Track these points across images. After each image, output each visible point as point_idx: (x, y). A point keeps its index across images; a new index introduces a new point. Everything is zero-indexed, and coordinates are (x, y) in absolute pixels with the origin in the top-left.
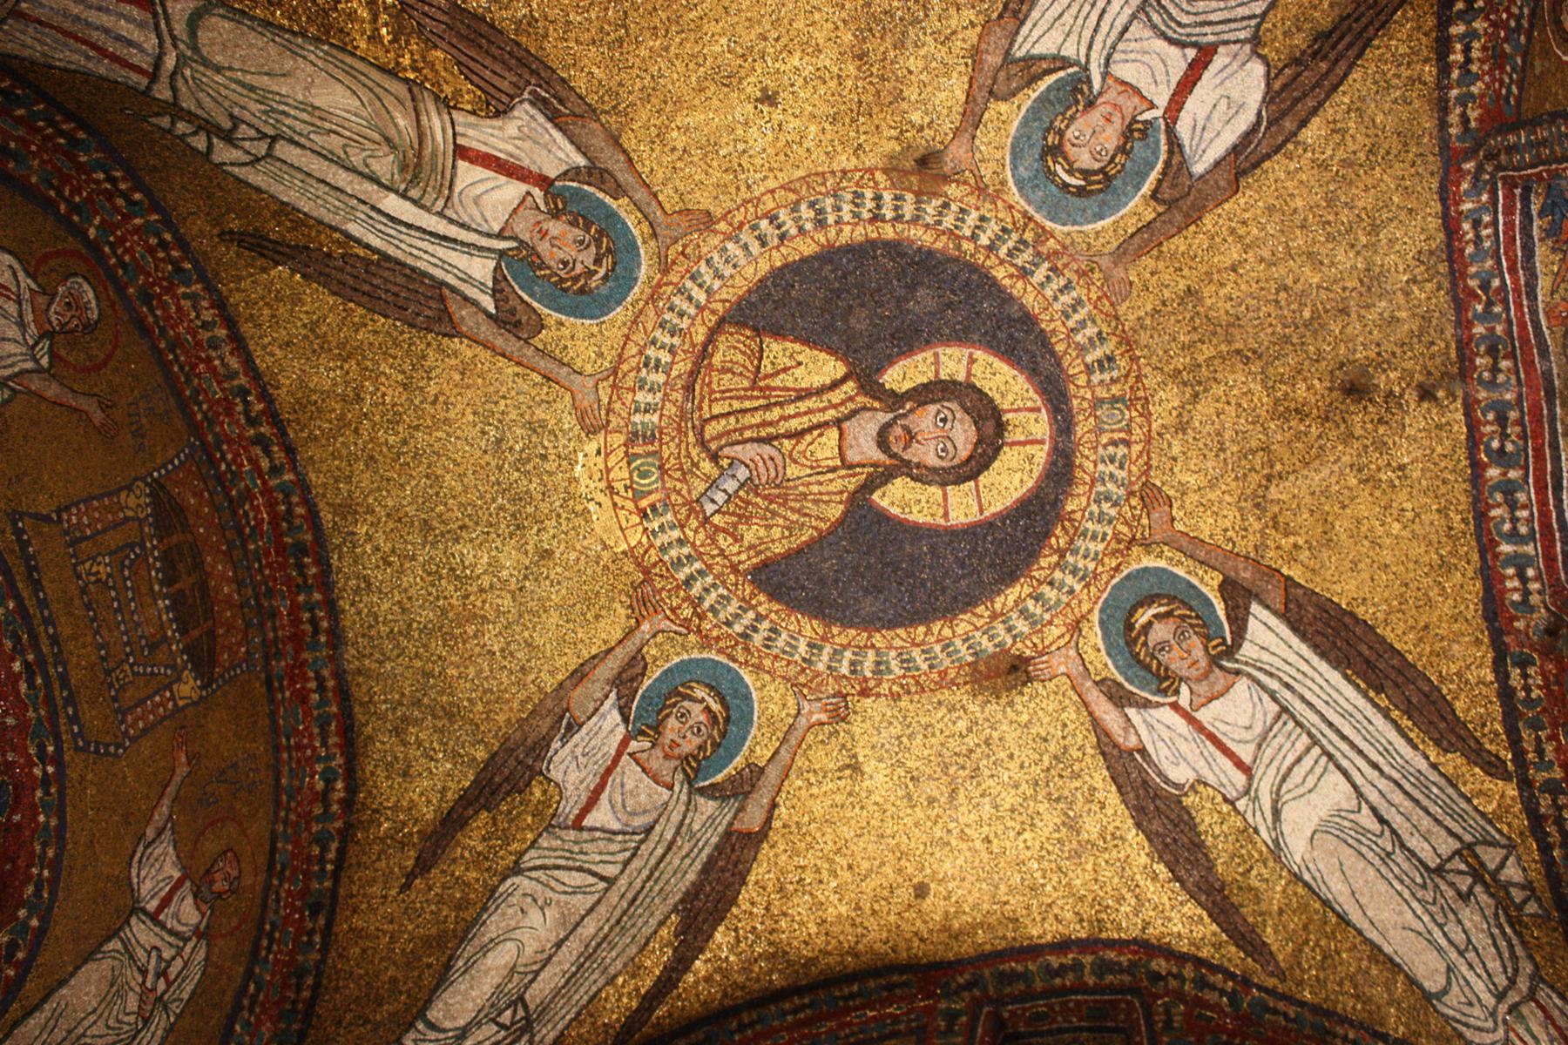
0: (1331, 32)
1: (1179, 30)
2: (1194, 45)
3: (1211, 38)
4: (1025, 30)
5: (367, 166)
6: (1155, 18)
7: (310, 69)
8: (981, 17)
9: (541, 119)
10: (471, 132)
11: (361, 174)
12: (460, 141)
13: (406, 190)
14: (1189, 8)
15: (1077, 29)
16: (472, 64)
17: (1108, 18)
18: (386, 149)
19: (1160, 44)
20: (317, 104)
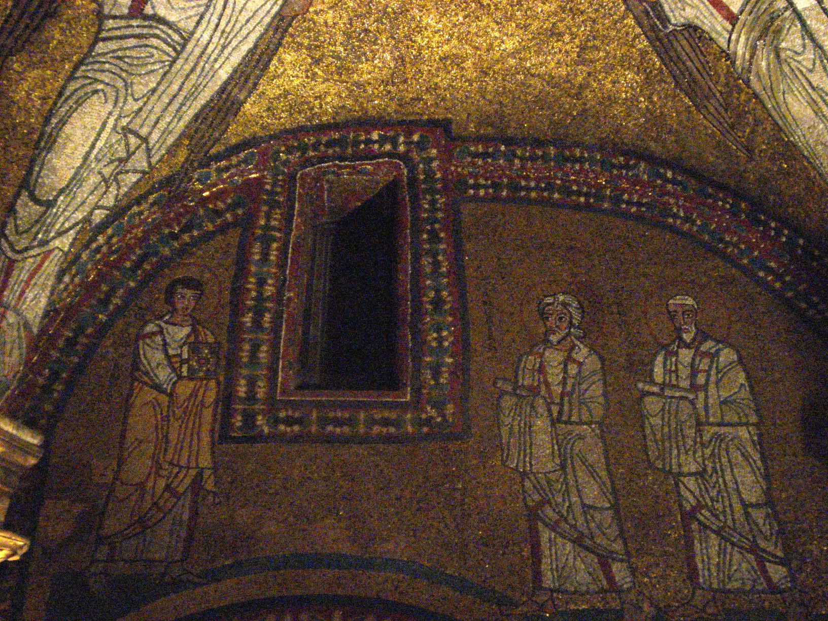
0: (44, 18)
1: (158, 32)
2: (146, 18)
3: (134, 23)
4: (276, 9)
5: (804, 46)
6: (176, 37)
7: (808, 136)
8: (309, 16)
9: (666, 7)
10: (719, 28)
11: (813, 40)
12: (730, 27)
13: (786, 9)
14: (151, 50)
15: (236, 14)
16: (700, 68)
17: (212, 26)
18: (783, 55)
19: (172, 17)
20: (813, 115)
